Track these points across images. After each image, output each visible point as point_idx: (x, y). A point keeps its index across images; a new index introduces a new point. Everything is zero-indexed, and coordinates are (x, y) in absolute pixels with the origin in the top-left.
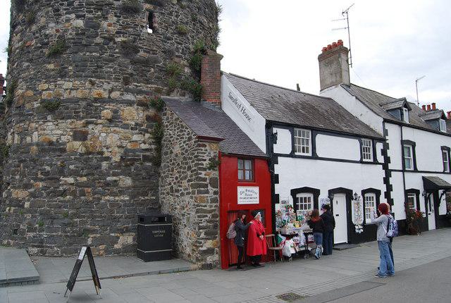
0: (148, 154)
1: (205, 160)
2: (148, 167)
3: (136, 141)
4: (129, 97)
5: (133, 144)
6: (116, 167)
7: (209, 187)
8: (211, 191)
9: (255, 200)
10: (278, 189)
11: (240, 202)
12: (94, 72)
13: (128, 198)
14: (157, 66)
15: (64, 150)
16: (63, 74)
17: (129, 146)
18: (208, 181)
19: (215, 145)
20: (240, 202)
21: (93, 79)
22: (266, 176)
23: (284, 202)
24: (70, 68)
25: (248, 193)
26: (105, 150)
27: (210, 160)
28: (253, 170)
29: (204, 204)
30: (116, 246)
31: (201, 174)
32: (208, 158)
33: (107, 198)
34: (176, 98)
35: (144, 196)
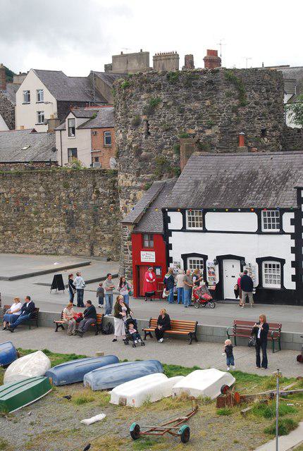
10: (171, 253)
11: (142, 260)
20: (142, 260)
22: (162, 243)
32: (128, 234)
34: (164, 181)
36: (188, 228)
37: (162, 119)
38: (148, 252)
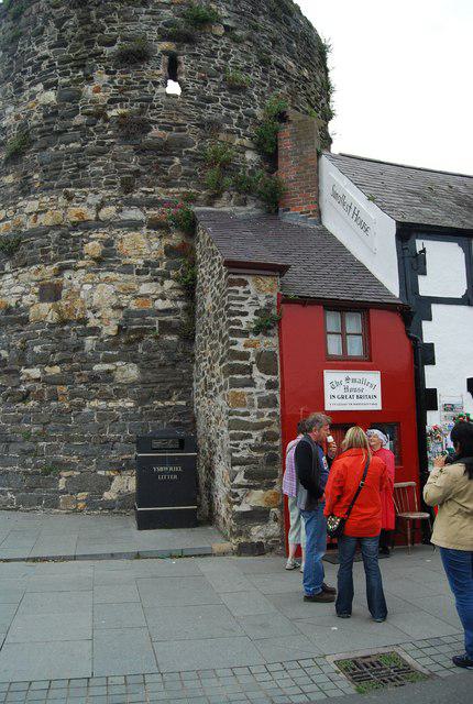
0: (170, 318)
1: (245, 314)
2: (168, 347)
3: (147, 296)
4: (134, 214)
5: (140, 300)
6: (114, 345)
7: (256, 373)
8: (259, 382)
9: (373, 401)
10: (432, 377)
12: (72, 177)
13: (131, 404)
14: (187, 152)
15: (25, 321)
16: (25, 189)
17: (133, 305)
18: (252, 359)
19: (269, 281)
21: (70, 190)
23: (449, 408)
24: (36, 176)
25: (351, 385)
26: (90, 314)
27: (256, 313)
28: (367, 335)
29: (242, 410)
30: (107, 495)
31: (235, 343)
32: (251, 310)
33: (94, 403)
34: (226, 209)
35: (163, 400)
37: (218, 62)
38: (353, 374)
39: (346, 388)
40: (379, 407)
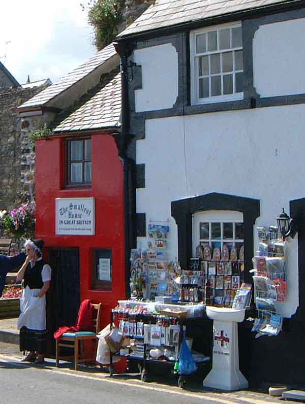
1: (28, 151)
9: (87, 226)
25: (74, 212)
36: (196, 99)
39: (70, 215)
40: (91, 233)
